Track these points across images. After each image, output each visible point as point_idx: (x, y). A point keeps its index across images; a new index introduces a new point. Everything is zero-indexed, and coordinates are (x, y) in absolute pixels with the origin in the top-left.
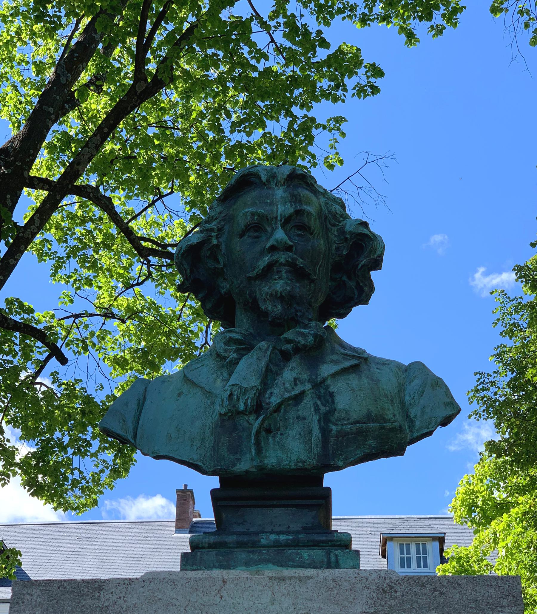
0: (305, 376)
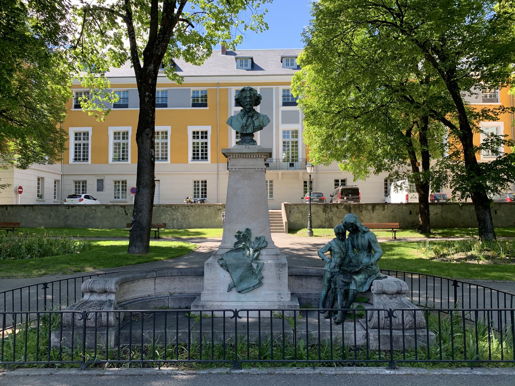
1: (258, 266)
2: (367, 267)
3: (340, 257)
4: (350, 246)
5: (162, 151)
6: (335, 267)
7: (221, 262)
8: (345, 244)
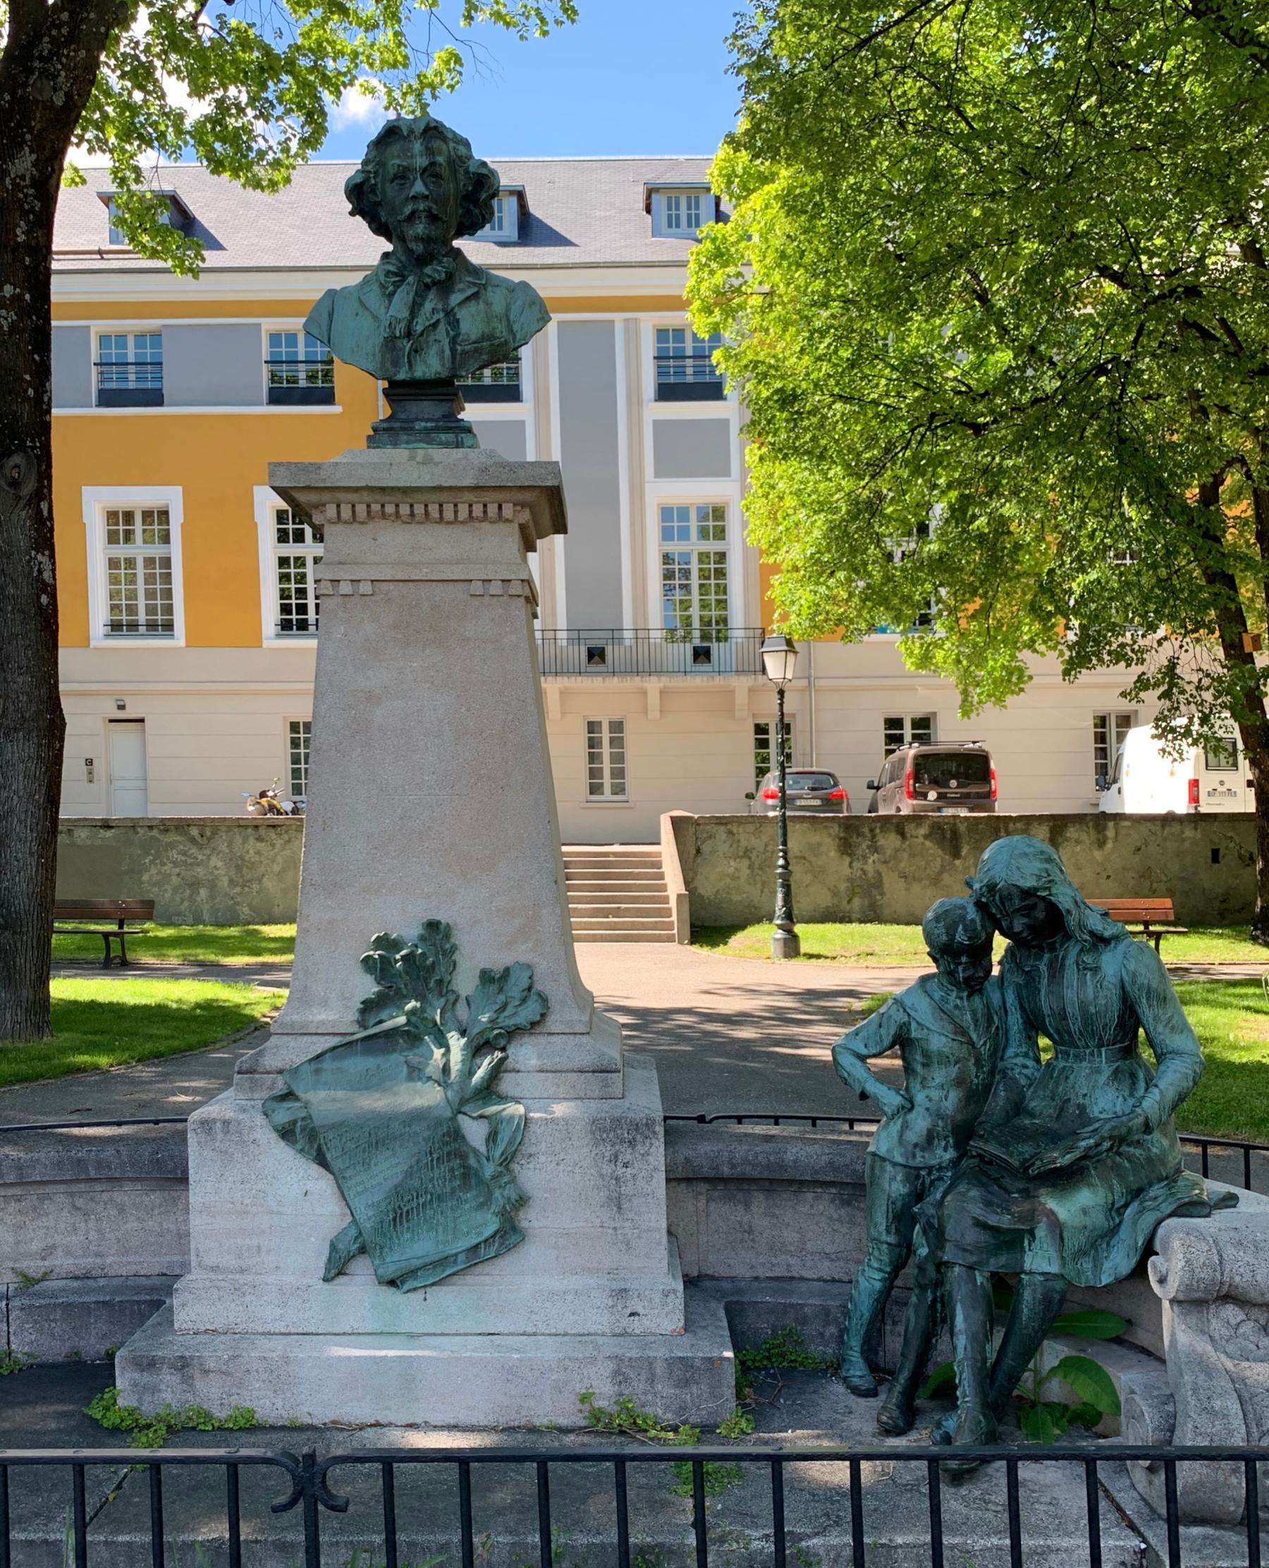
0: (440, 306)
1: (492, 1137)
2: (1120, 1140)
3: (959, 1082)
4: (1015, 1020)
5: (150, 595)
6: (930, 1137)
7: (283, 1115)
8: (988, 1006)
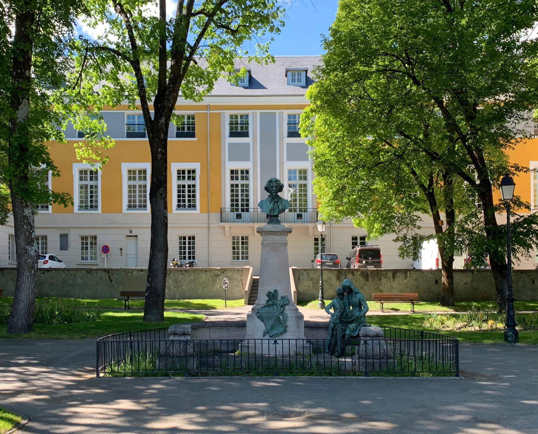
1: (283, 318)
2: (358, 318)
4: (347, 304)
6: (336, 319)
7: (258, 315)
